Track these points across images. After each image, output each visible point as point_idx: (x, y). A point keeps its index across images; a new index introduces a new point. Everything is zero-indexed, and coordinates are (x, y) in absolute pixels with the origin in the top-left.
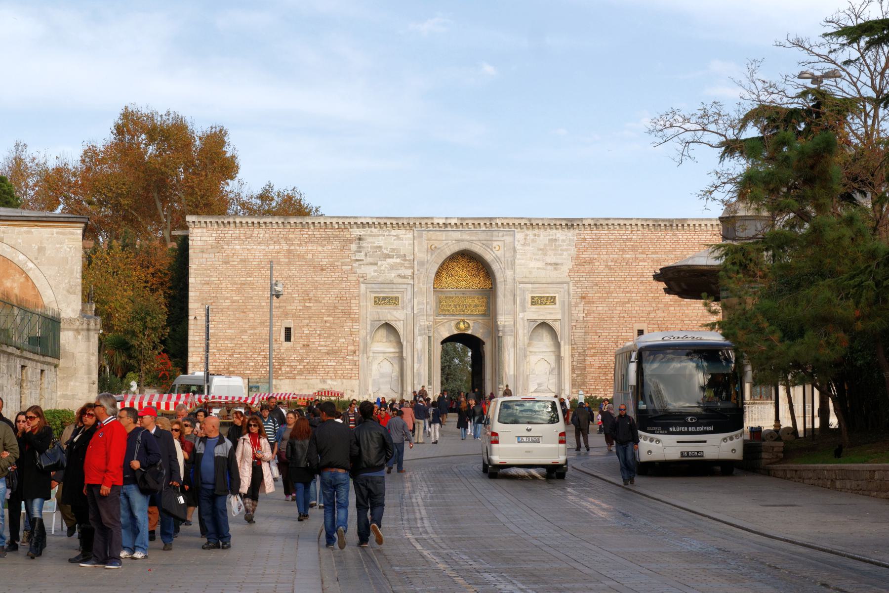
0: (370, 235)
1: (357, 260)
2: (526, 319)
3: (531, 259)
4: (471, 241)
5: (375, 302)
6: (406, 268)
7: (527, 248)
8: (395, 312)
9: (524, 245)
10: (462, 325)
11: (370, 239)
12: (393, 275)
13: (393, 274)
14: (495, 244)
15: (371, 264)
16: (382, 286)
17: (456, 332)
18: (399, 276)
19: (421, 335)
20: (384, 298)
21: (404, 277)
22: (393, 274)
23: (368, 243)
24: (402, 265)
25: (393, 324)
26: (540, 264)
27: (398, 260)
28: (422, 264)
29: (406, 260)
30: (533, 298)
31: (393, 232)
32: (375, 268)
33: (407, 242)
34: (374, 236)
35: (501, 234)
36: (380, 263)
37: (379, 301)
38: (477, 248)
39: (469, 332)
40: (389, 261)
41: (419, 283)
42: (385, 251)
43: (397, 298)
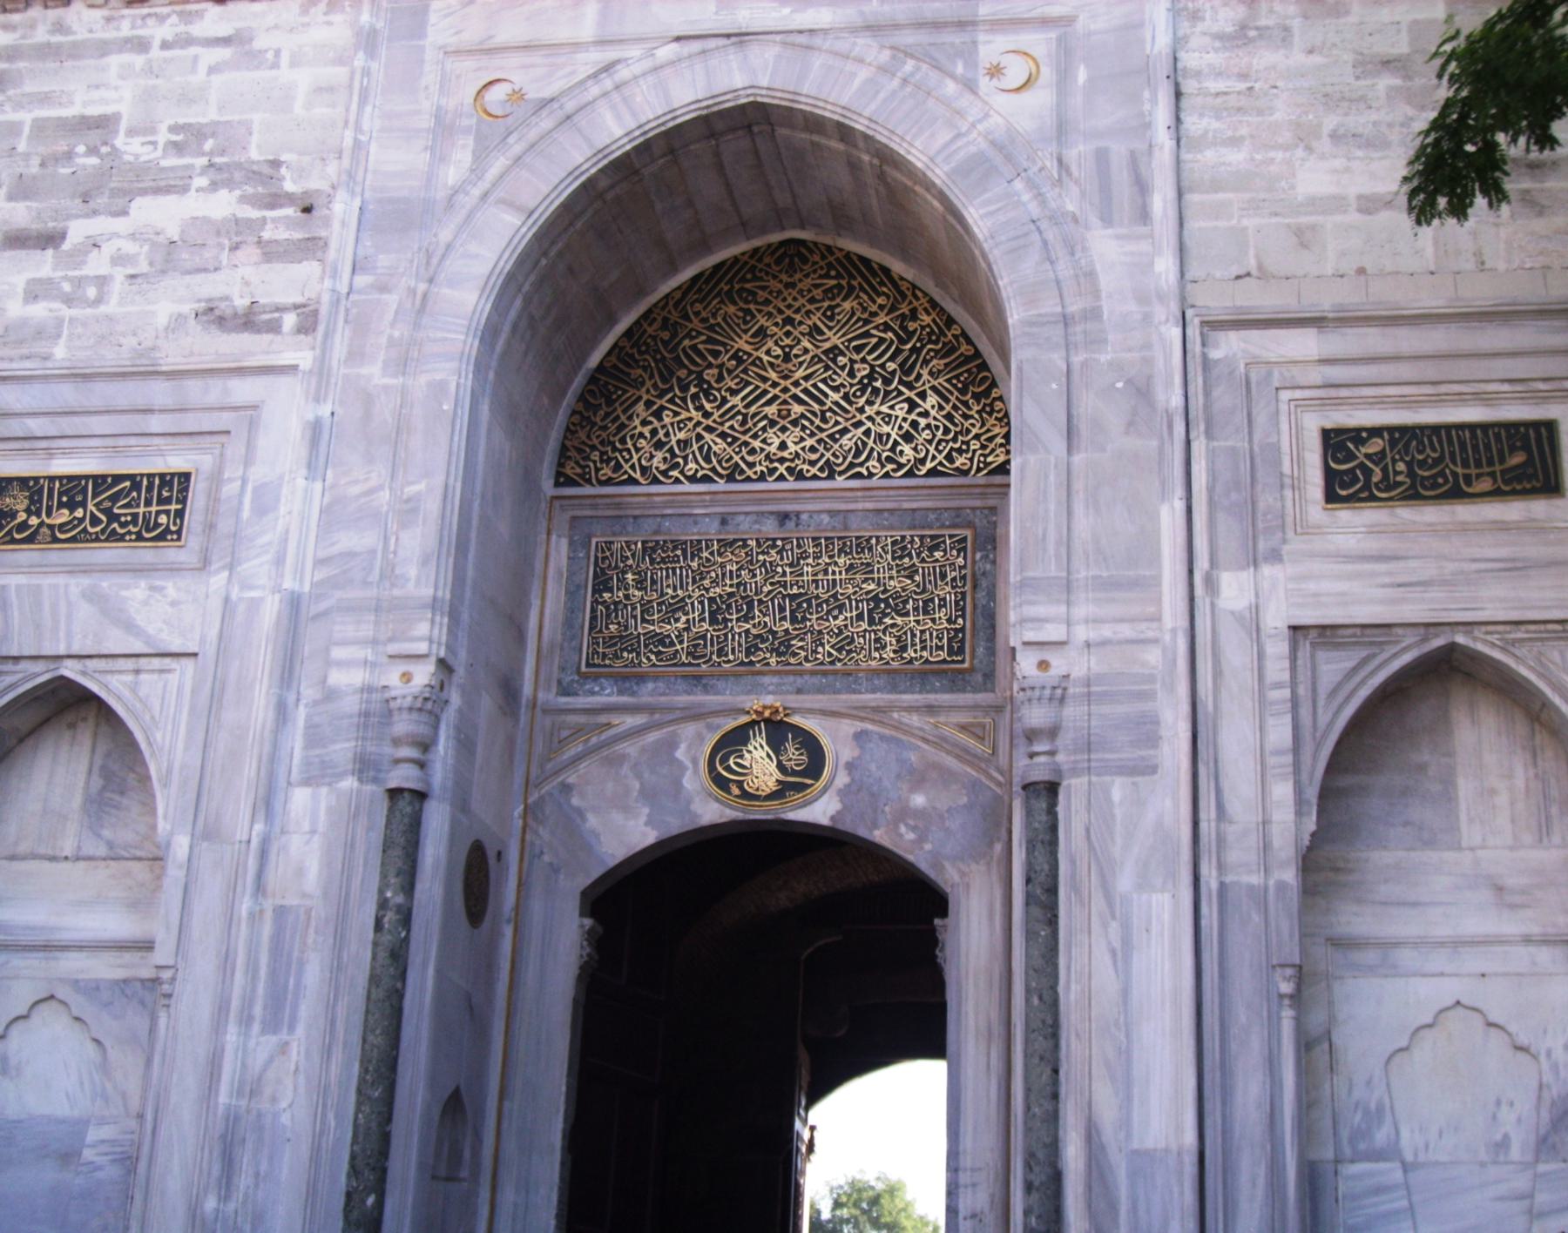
0: (47, 52)
2: (1276, 618)
3: (1305, 137)
4: (800, 40)
6: (272, 253)
7: (1265, 58)
8: (135, 593)
9: (1241, 37)
10: (761, 765)
12: (163, 311)
13: (170, 301)
16: (68, 394)
17: (711, 811)
18: (215, 317)
19: (316, 775)
20: (73, 489)
21: (249, 321)
22: (170, 301)
25: (112, 687)
27: (223, 205)
28: (394, 217)
29: (276, 200)
30: (1336, 442)
32: (43, 264)
33: (303, 79)
36: (78, 231)
39: (820, 810)
41: (356, 355)
42: (132, 148)
43: (176, 485)
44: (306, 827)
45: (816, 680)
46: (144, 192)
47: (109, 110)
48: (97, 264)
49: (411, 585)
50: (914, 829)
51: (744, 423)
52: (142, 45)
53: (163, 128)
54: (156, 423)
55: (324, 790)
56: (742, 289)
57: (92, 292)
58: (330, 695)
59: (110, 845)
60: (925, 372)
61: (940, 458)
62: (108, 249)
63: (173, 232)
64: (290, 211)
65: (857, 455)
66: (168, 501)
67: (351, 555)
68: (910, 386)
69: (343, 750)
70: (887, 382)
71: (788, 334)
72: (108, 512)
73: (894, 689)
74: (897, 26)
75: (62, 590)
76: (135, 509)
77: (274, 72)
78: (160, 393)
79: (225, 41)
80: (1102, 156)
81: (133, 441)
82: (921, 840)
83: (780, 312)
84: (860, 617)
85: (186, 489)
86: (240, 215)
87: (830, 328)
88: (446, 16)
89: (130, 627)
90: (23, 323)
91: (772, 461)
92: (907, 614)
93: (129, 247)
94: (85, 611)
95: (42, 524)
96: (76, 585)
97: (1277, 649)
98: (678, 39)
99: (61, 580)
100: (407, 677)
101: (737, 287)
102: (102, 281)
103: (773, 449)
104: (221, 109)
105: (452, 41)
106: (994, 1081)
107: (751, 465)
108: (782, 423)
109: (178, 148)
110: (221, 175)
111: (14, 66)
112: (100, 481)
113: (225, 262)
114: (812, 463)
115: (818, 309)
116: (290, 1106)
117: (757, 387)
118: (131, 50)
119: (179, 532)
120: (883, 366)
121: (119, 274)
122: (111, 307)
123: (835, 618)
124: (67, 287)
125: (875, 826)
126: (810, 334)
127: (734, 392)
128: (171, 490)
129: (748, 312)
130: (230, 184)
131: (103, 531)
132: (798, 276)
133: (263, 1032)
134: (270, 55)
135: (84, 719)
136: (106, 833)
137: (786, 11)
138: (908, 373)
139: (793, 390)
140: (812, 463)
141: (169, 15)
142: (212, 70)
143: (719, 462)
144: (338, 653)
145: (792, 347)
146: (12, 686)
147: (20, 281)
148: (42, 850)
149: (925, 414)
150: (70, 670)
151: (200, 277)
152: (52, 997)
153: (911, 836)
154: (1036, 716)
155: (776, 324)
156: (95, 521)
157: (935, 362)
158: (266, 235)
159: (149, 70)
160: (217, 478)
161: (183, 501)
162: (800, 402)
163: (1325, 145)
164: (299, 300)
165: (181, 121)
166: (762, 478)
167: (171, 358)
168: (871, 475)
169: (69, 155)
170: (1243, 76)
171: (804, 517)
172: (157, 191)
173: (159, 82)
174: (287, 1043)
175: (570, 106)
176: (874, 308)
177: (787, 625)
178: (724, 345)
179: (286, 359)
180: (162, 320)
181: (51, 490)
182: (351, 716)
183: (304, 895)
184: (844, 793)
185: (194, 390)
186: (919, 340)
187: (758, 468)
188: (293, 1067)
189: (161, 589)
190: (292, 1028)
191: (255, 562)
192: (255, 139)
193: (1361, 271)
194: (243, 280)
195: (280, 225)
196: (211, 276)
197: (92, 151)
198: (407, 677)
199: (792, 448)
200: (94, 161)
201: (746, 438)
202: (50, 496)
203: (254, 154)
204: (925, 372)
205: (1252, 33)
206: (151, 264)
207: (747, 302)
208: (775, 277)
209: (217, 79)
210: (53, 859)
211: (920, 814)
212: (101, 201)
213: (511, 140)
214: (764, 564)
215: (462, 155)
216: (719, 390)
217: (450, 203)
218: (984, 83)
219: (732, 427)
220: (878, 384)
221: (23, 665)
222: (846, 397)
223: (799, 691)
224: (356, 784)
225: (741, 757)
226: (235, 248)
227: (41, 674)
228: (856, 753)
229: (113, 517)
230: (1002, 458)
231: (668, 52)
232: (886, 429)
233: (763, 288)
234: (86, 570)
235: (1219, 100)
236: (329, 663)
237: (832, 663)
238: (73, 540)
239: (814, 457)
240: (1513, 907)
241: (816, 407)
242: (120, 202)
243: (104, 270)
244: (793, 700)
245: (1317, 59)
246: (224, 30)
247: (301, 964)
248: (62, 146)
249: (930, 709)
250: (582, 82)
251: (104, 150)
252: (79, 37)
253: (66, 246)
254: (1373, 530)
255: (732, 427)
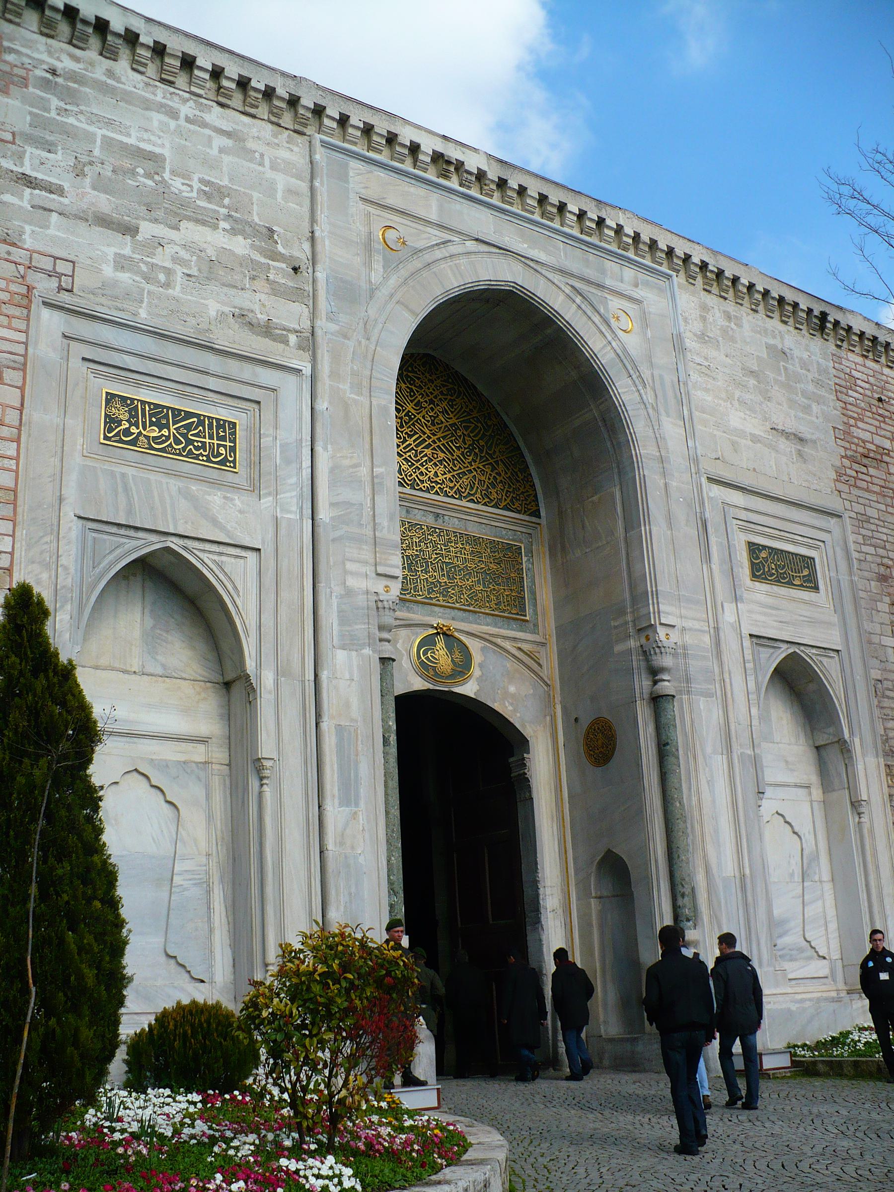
1: (29, 182)
5: (111, 422)
6: (276, 290)
8: (215, 499)
10: (442, 656)
11: (101, 107)
12: (213, 308)
14: (615, 304)
15: (103, 221)
19: (349, 643)
21: (267, 330)
23: (94, 119)
24: (256, 271)
25: (205, 561)
26: (754, 426)
27: (240, 246)
29: (275, 256)
31: (215, 116)
34: (127, 98)
35: (629, 273)
36: (147, 229)
37: (128, 424)
38: (555, 298)
39: (469, 689)
40: (190, 231)
41: (334, 374)
43: (226, 429)
44: (347, 676)
45: (460, 613)
46: (189, 219)
47: (157, 150)
48: (162, 258)
49: (385, 531)
50: (512, 704)
51: (416, 456)
52: (173, 114)
53: (195, 177)
54: (212, 383)
55: (354, 653)
56: (407, 376)
57: (162, 277)
58: (349, 593)
59: (164, 666)
60: (497, 450)
61: (508, 500)
62: (170, 250)
63: (211, 252)
64: (284, 266)
65: (472, 488)
66: (223, 439)
67: (348, 504)
68: (492, 458)
69: (360, 629)
70: (481, 451)
71: (432, 409)
72: (185, 436)
73: (496, 626)
74: (572, 275)
75: (165, 486)
76: (203, 442)
77: (260, 168)
78: (212, 362)
79: (228, 134)
80: (661, 377)
81: (196, 390)
82: (515, 710)
83: (428, 396)
84: (479, 581)
85: (235, 433)
86: (253, 257)
87: (452, 412)
88: (359, 174)
89: (215, 522)
90: (115, 283)
91: (432, 482)
92: (499, 585)
93: (183, 254)
94: (183, 504)
95: (140, 434)
96: (174, 484)
97: (747, 643)
98: (477, 240)
99: (165, 480)
100: (387, 589)
101: (405, 373)
102: (168, 272)
103: (431, 475)
104: (231, 180)
105: (365, 193)
106: (556, 843)
107: (422, 482)
108: (435, 461)
109: (208, 197)
110: (240, 227)
111: (81, 88)
112: (176, 412)
113: (247, 286)
114: (451, 488)
115: (446, 399)
116: (363, 852)
117: (420, 436)
118: (166, 113)
119: (234, 462)
120: (478, 441)
121: (179, 271)
122: (176, 292)
123: (468, 580)
124: (144, 268)
125: (494, 701)
126: (442, 412)
127: (410, 436)
128: (225, 431)
129: (412, 390)
130: (242, 233)
131: (184, 449)
132: (434, 377)
133: (341, 805)
134: (257, 155)
135: (134, 575)
136: (159, 658)
137: (526, 246)
138: (490, 448)
139: (438, 443)
140: (451, 488)
141: (188, 100)
142: (221, 150)
143: (406, 475)
144: (349, 566)
145: (435, 418)
146: (137, 548)
147: (111, 251)
148: (117, 665)
149: (499, 474)
150: (174, 544)
151: (233, 291)
152: (136, 770)
153: (510, 708)
154: (667, 661)
155: (426, 402)
156: (178, 442)
157: (501, 446)
158: (271, 277)
159: (179, 132)
160: (255, 432)
161: (234, 441)
162: (443, 452)
163: (736, 403)
164: (297, 327)
165: (207, 178)
166: (428, 491)
167: (222, 340)
168: (478, 503)
169: (133, 173)
170: (706, 359)
171: (446, 517)
172: (197, 221)
173: (187, 143)
174: (355, 813)
175: (428, 257)
176: (471, 407)
177: (446, 580)
178: (402, 407)
179: (295, 364)
180: (213, 313)
181: (143, 410)
182: (363, 609)
183: (352, 720)
184: (480, 680)
185: (233, 367)
186: (493, 431)
187: (425, 484)
188: (361, 828)
189: (232, 500)
190: (357, 805)
191: (288, 495)
192: (255, 207)
193: (754, 470)
194: (260, 303)
195: (279, 272)
196: (240, 293)
197: (148, 176)
198: (387, 589)
199: (441, 477)
200: (150, 183)
201: (417, 465)
202: (144, 415)
203: (256, 219)
204: (497, 450)
205: (707, 338)
206: (199, 270)
207: (411, 384)
208: (423, 374)
209: (227, 159)
210: (125, 672)
211: (513, 696)
212: (160, 214)
213: (401, 266)
214: (431, 542)
215: (378, 265)
216: (402, 432)
217: (372, 292)
218: (613, 322)
219: (410, 456)
220: (477, 451)
221: (140, 534)
222: (463, 454)
223: (453, 619)
224: (371, 652)
225: (434, 653)
226: (253, 278)
227: (155, 544)
228: (483, 659)
229: (189, 442)
230: (534, 508)
231: (471, 245)
232: (483, 478)
233: (418, 378)
234: (177, 475)
235: (699, 367)
236: (346, 572)
237: (468, 605)
238: (163, 450)
239: (452, 485)
240: (792, 770)
241: (450, 456)
242: (174, 221)
243: (168, 264)
244: (454, 625)
245: (728, 360)
246: (225, 126)
247: (357, 763)
248: (127, 163)
249: (515, 639)
250: (433, 246)
251: (157, 177)
252: (126, 87)
253: (139, 237)
254: (768, 594)
255: (410, 456)
